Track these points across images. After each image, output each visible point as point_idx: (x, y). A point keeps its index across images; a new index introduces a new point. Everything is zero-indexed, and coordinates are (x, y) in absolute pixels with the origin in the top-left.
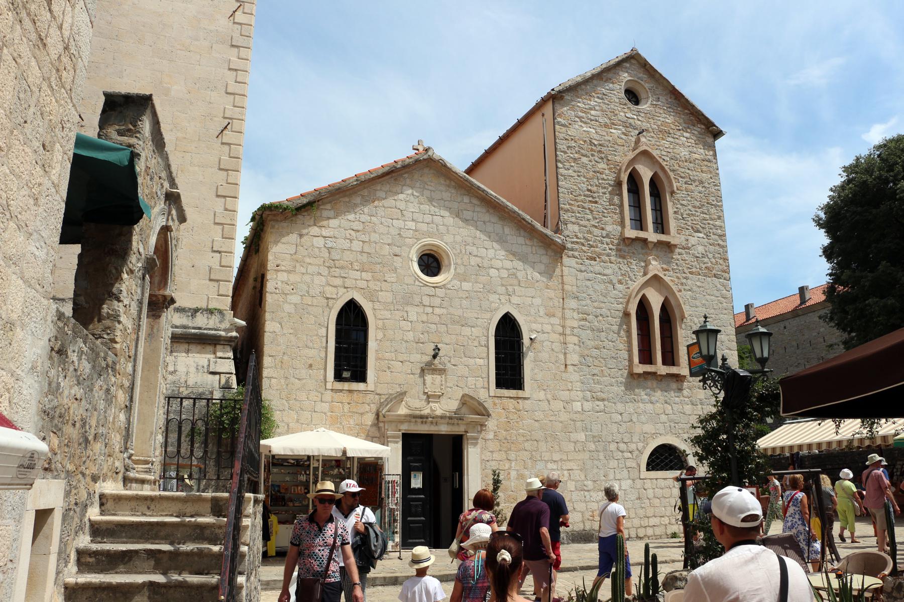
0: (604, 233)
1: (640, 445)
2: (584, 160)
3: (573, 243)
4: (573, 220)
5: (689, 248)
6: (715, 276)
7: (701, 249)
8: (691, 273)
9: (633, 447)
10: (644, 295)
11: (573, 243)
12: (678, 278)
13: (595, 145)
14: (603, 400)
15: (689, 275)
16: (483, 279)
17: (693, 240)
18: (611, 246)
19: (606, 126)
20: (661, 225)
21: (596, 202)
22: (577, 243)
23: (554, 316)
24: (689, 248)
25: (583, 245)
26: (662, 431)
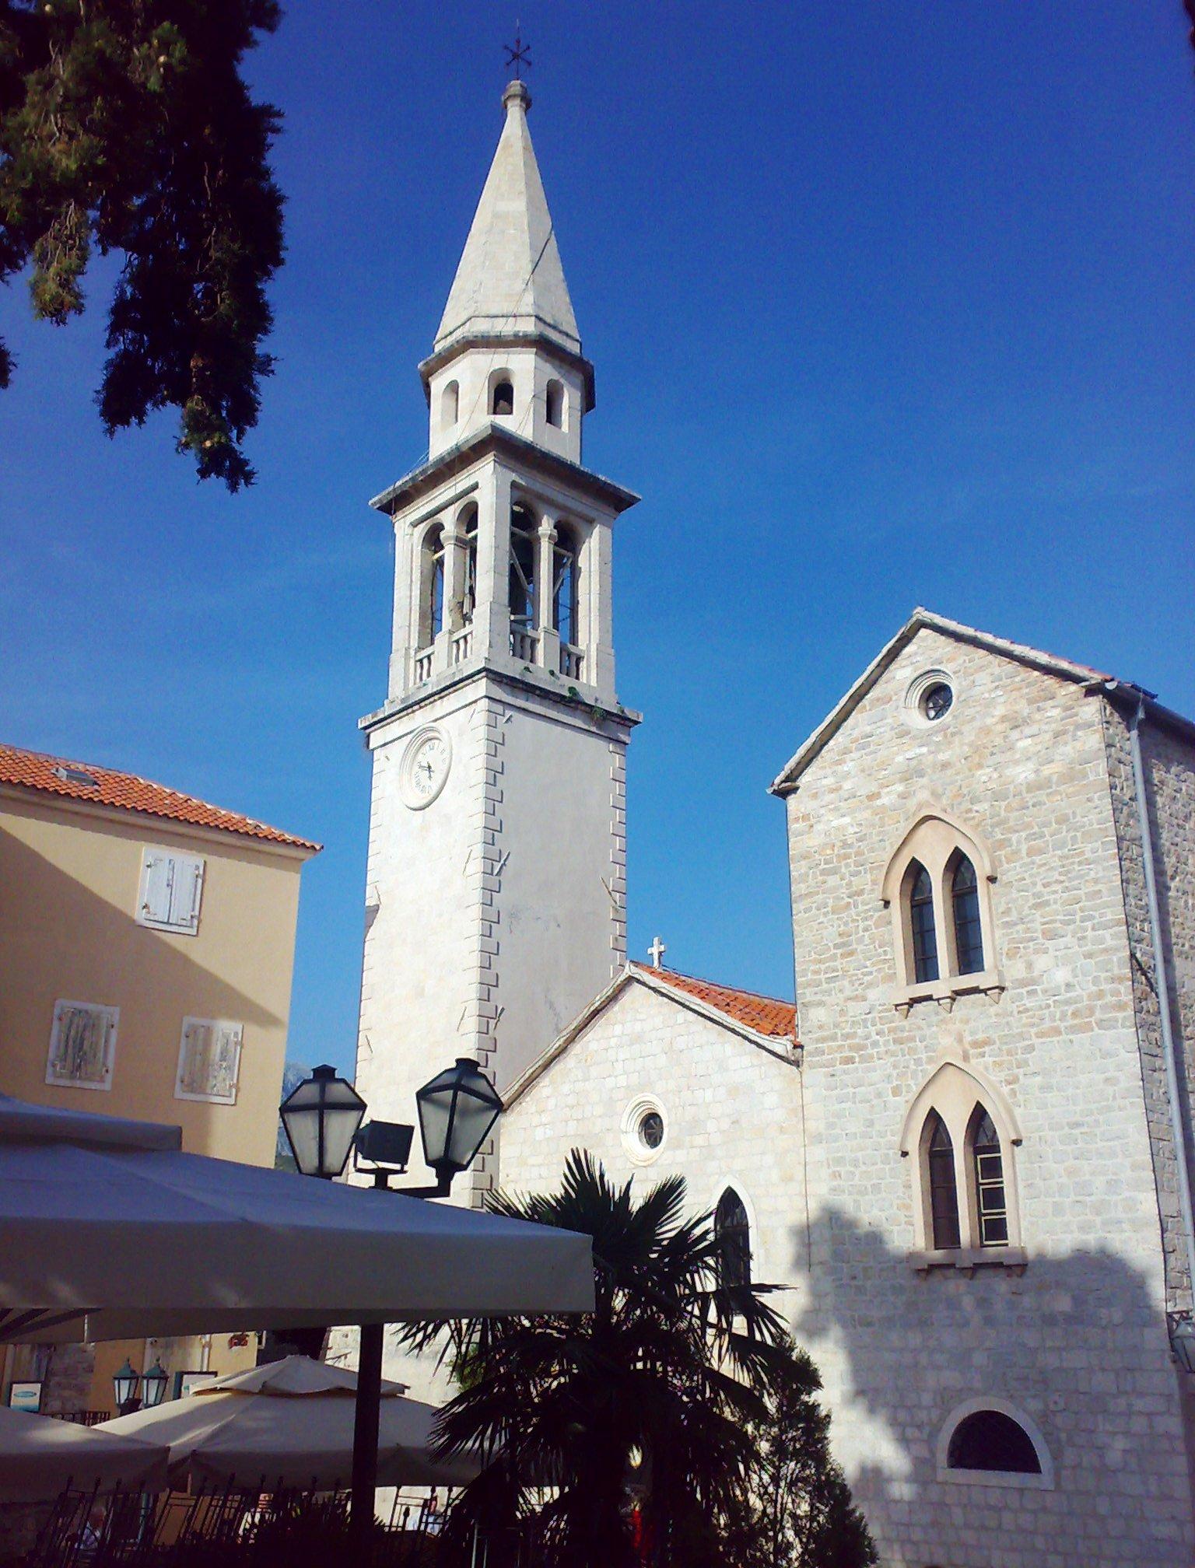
0: (864, 1006)
1: (935, 1415)
2: (832, 881)
3: (818, 1041)
4: (818, 998)
5: (1033, 981)
6: (1101, 1024)
7: (1061, 976)
8: (1040, 1035)
9: (923, 1416)
10: (932, 1109)
11: (818, 1041)
12: (1009, 1053)
13: (851, 846)
14: (870, 1324)
15: (1036, 1041)
16: (699, 1140)
17: (1042, 962)
18: (879, 1026)
19: (872, 797)
20: (969, 957)
21: (851, 954)
22: (824, 1040)
23: (791, 1179)
24: (1033, 981)
25: (834, 1038)
26: (977, 1385)
